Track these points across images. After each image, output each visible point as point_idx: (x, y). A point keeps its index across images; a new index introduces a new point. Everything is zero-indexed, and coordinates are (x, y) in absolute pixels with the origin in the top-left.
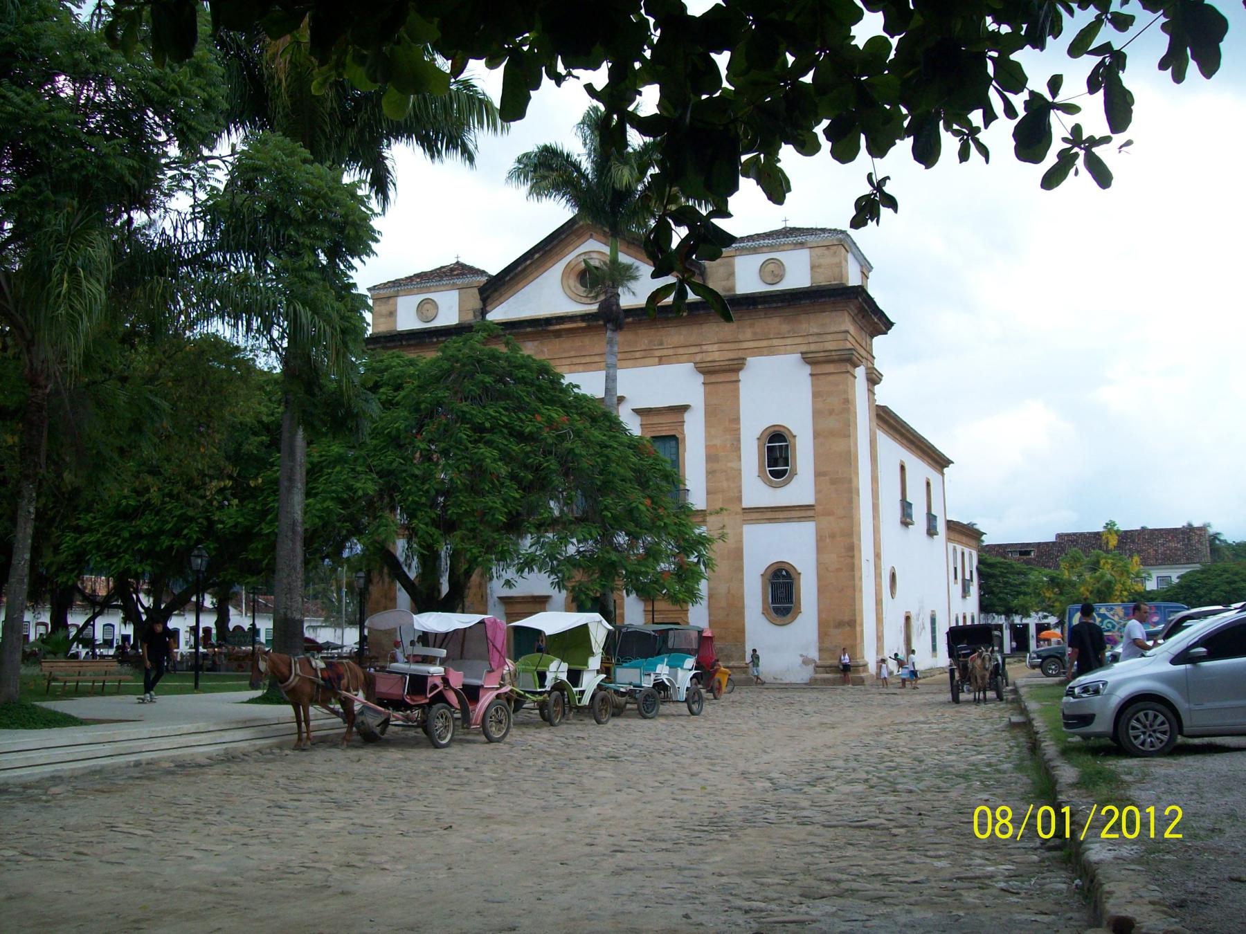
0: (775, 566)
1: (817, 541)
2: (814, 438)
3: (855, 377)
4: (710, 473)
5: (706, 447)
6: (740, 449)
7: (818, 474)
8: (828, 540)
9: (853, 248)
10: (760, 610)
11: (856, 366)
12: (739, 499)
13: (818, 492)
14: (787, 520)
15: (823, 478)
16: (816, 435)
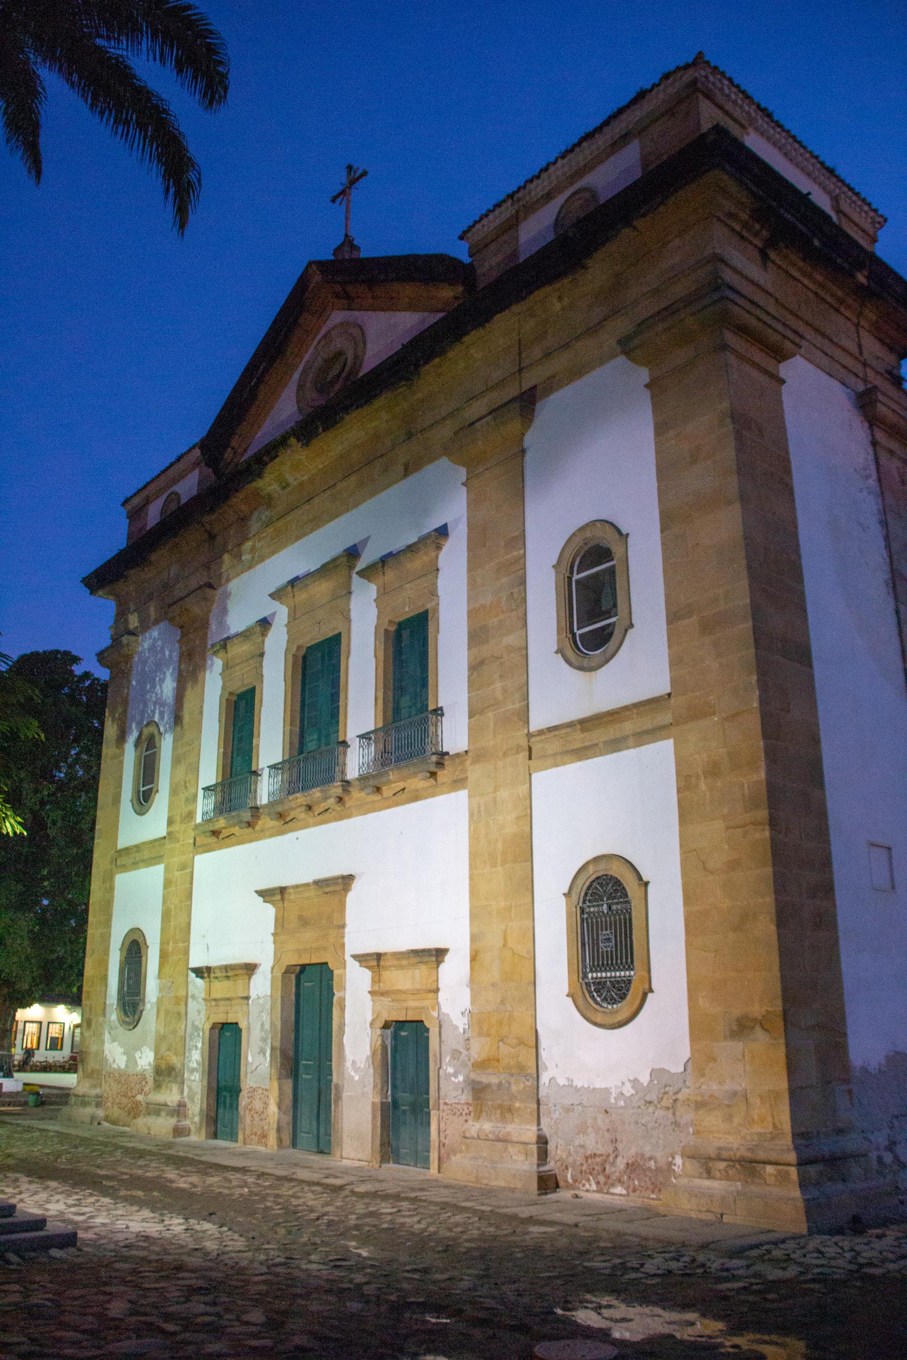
0: (591, 869)
1: (679, 790)
2: (662, 532)
3: (783, 382)
4: (475, 667)
5: (472, 614)
6: (524, 600)
7: (673, 617)
8: (703, 786)
9: (761, 121)
10: (566, 989)
11: (780, 355)
12: (524, 715)
13: (675, 662)
14: (615, 745)
15: (685, 622)
16: (667, 520)
